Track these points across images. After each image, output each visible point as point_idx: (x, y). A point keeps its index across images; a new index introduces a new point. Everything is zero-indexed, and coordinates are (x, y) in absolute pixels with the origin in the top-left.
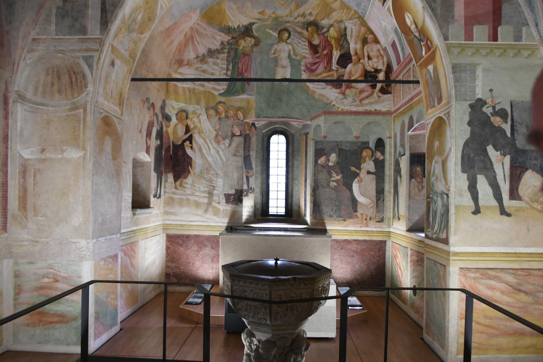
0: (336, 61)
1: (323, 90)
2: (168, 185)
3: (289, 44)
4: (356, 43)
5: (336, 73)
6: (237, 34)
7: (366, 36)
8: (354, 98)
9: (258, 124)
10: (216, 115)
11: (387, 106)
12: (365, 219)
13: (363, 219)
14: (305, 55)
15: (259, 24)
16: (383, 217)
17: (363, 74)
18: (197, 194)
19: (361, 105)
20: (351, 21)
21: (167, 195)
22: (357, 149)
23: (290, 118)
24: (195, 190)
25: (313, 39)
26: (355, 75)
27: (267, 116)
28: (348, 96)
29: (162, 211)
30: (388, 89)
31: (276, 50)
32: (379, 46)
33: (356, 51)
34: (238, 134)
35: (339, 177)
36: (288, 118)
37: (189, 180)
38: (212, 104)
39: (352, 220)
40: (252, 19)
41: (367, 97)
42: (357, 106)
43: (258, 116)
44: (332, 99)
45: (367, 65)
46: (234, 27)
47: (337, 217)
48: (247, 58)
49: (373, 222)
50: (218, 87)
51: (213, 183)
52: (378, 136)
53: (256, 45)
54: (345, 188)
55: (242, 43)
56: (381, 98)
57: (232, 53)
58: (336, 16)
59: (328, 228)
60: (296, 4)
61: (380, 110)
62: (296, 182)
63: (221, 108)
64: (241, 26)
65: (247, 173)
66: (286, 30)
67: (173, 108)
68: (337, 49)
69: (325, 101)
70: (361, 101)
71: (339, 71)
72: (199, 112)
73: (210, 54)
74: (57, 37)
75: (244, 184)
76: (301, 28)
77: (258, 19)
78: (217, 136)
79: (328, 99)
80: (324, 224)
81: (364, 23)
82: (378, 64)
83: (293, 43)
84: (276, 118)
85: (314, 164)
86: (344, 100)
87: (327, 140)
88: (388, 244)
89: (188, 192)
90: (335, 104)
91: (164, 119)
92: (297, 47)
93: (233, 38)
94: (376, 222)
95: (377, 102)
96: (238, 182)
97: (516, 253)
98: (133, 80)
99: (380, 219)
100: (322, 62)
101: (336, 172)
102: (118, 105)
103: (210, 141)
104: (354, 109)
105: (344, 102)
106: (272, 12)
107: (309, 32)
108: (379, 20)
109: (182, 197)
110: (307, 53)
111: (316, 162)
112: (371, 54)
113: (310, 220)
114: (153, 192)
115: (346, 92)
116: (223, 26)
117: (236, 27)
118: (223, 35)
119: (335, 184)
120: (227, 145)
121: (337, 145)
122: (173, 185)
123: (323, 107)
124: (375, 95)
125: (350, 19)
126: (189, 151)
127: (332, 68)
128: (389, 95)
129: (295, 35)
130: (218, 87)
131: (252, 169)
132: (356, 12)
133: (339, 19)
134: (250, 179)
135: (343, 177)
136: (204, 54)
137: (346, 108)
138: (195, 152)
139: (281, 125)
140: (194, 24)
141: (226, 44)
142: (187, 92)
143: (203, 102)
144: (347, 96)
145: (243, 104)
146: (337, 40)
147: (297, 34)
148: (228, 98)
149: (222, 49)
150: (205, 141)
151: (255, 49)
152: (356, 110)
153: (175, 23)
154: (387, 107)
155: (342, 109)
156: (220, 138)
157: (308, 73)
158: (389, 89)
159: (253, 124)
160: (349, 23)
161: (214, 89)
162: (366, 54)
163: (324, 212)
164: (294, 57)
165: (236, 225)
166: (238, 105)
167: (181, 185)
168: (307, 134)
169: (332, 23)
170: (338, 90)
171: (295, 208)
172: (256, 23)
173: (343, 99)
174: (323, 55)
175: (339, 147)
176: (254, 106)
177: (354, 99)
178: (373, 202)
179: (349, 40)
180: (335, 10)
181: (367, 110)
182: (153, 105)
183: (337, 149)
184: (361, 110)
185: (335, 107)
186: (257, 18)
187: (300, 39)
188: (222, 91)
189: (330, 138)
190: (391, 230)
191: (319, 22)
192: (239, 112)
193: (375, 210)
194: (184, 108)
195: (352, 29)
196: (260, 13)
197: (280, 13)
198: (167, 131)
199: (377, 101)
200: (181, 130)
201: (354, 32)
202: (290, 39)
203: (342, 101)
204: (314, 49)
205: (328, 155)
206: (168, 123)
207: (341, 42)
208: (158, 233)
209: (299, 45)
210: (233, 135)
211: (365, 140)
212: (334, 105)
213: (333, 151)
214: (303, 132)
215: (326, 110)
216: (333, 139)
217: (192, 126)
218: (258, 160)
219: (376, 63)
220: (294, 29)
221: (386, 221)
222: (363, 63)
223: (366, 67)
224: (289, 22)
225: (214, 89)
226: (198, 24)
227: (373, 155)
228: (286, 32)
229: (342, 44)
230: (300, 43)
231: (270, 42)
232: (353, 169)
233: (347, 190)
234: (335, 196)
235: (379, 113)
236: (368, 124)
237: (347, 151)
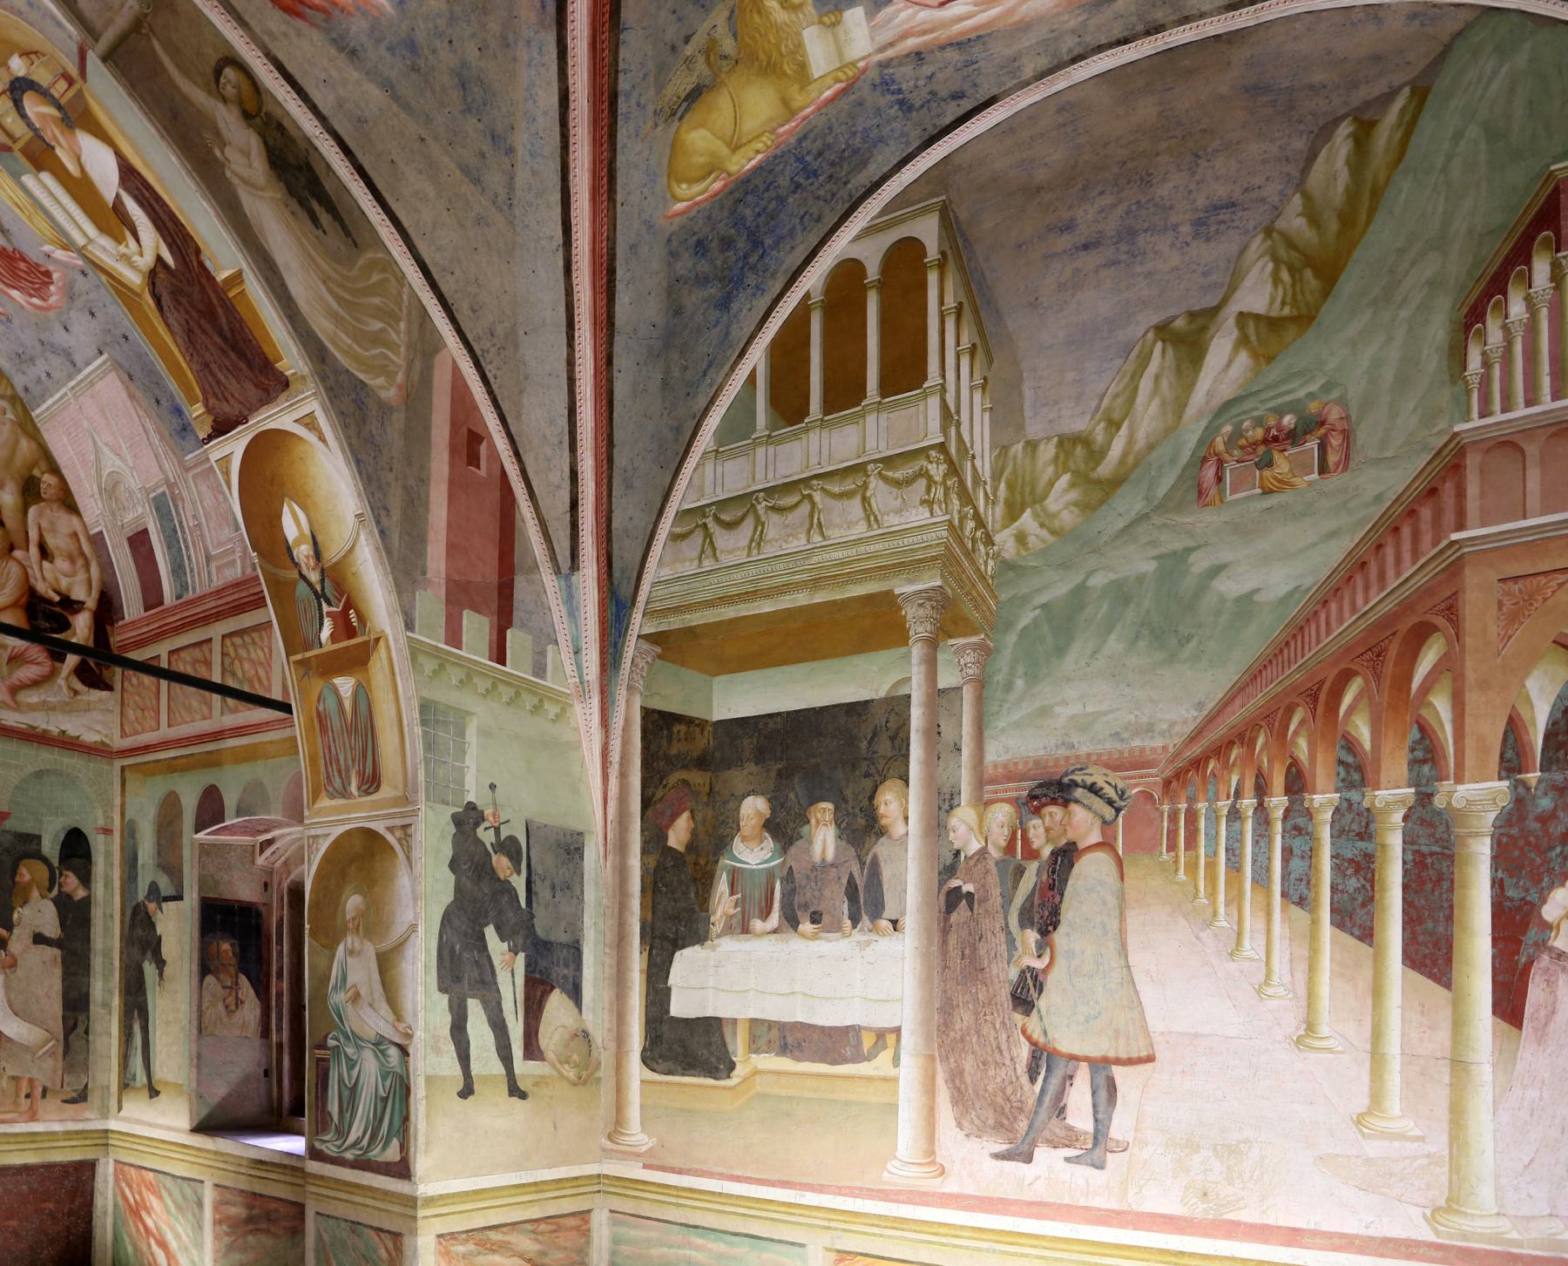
12: (28, 1096)
13: (17, 1096)
16: (86, 1086)
41: (35, 684)
45: (38, 575)
49: (52, 1105)
70: (14, 690)
88: (100, 1170)
94: (65, 1101)
97: (535, 1184)
108: (95, 442)
112: (51, 542)
178: (53, 1036)
184: (15, 724)
190: (113, 1125)
193: (60, 1064)
211: (28, 827)
221: (94, 1097)
223: (32, 580)
235: (71, 744)
236: (39, 774)
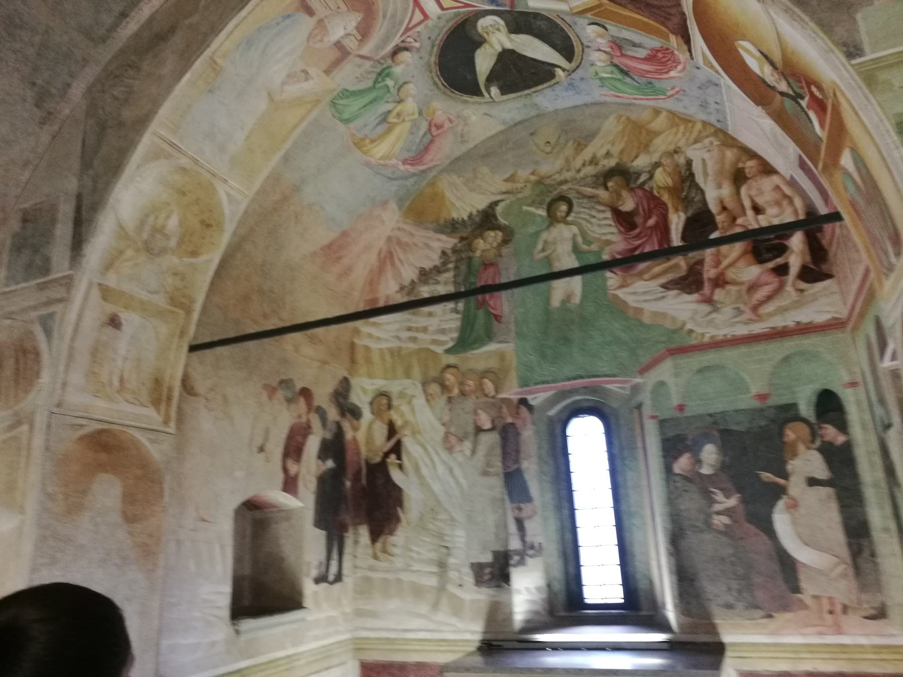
0: (680, 235)
2: (360, 551)
3: (572, 223)
4: (719, 186)
6: (469, 229)
7: (740, 165)
8: (738, 305)
9: (536, 399)
10: (443, 393)
11: (828, 309)
14: (609, 237)
15: (508, 202)
18: (416, 567)
20: (698, 145)
21: (360, 573)
22: (767, 426)
23: (594, 376)
24: (412, 558)
25: (620, 203)
27: (544, 379)
28: (722, 303)
29: (348, 609)
31: (546, 242)
32: (775, 179)
33: (722, 202)
34: (488, 425)
35: (733, 502)
36: (589, 377)
37: (399, 538)
38: (433, 373)
39: (788, 615)
40: (493, 194)
41: (769, 298)
42: (749, 323)
43: (524, 383)
46: (463, 219)
47: (747, 608)
48: (491, 270)
49: (853, 620)
50: (443, 338)
51: (445, 541)
52: (818, 386)
53: (506, 242)
54: (752, 529)
55: (480, 245)
56: (806, 293)
57: (463, 268)
58: (661, 145)
59: (727, 638)
60: (577, 143)
62: (636, 521)
63: (450, 377)
64: (475, 213)
65: (517, 511)
66: (563, 198)
67: (364, 391)
68: (677, 210)
69: (668, 325)
70: (755, 309)
72: (409, 392)
73: (423, 278)
74: (7, 289)
75: (511, 537)
76: (592, 188)
77: (505, 193)
78: (447, 435)
79: (674, 319)
80: (712, 629)
81: (728, 141)
83: (580, 221)
84: (564, 380)
85: (663, 476)
86: (714, 315)
87: (688, 413)
89: (399, 563)
91: (348, 415)
92: (589, 225)
93: (462, 239)
94: (867, 618)
95: (797, 305)
96: (497, 535)
98: (193, 348)
99: (873, 608)
101: (721, 489)
102: (150, 405)
103: (434, 449)
104: (742, 330)
105: (716, 318)
106: (530, 171)
107: (610, 189)
109: (387, 576)
110: (612, 233)
111: (668, 469)
112: (760, 201)
113: (677, 621)
114: (314, 573)
115: (716, 297)
116: (442, 221)
117: (466, 218)
118: (443, 237)
119: (725, 520)
120: (468, 452)
121: (715, 423)
122: (370, 551)
123: (663, 339)
124: (789, 288)
125: (696, 141)
126: (396, 475)
128: (827, 283)
129: (581, 203)
130: (443, 338)
131: (528, 499)
132: (705, 124)
133: (672, 148)
134: (529, 525)
135: (743, 501)
136: (413, 281)
137: (721, 333)
138: (406, 474)
139: (586, 394)
140: (392, 230)
141: (449, 252)
142: (388, 357)
143: (416, 371)
144: (719, 306)
145: (493, 363)
146: (674, 191)
147: (585, 201)
148: (462, 355)
149: (444, 264)
150: (425, 449)
151: (505, 251)
152: (749, 333)
153: (344, 234)
155: (712, 337)
156: (453, 440)
157: (619, 273)
158: (824, 267)
159: (523, 402)
160: (695, 149)
161: (435, 342)
162: (747, 204)
163: (711, 597)
164: (585, 247)
165: (501, 637)
166: (481, 365)
167: (385, 551)
168: (639, 407)
169: (657, 161)
170: (695, 297)
171: (642, 585)
172: (502, 200)
175: (722, 427)
176: (514, 363)
177: (738, 309)
179: (702, 185)
180: (657, 134)
182: (306, 393)
183: (716, 434)
185: (694, 335)
186: (504, 190)
187: (593, 208)
188: (451, 344)
189: (695, 408)
191: (629, 165)
192: (486, 380)
194: (384, 389)
195: (704, 160)
196: (507, 180)
197: (546, 169)
198: (355, 440)
199: (796, 302)
200: (380, 432)
201: (710, 164)
202: (573, 214)
204: (625, 220)
205: (695, 450)
206: (355, 422)
207: (684, 193)
208: (335, 661)
209: (593, 220)
210: (479, 430)
211: (785, 400)
212: (691, 331)
213: (706, 437)
214: (634, 403)
215: (672, 346)
216: (701, 411)
217: (399, 422)
218: (544, 478)
219: (777, 216)
220: (578, 192)
224: (565, 182)
225: (435, 342)
226: (399, 229)
227: (814, 435)
228: (561, 203)
229: (686, 197)
230: (594, 217)
231: (531, 230)
232: (767, 476)
233: (762, 534)
234: (730, 551)
235: (806, 329)
236: (786, 359)
237: (742, 432)
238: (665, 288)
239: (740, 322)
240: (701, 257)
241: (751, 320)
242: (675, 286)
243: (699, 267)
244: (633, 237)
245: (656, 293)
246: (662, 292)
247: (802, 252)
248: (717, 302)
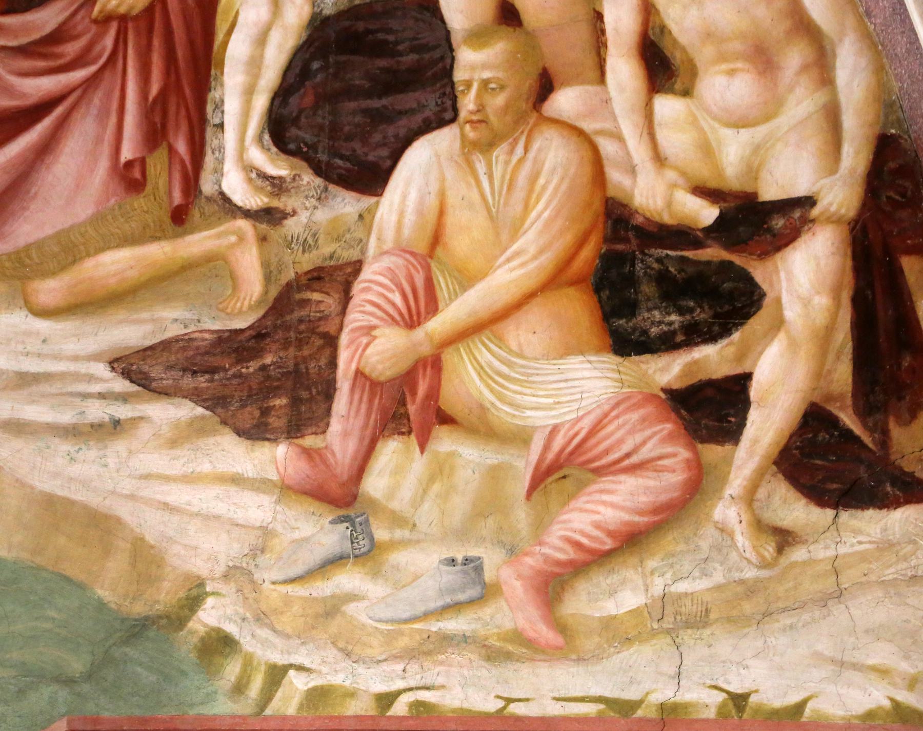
0: (261, 102)
1: (91, 453)
5: (263, 239)
8: (473, 552)
17: (588, 252)
19: (545, 634)
26: (481, 275)
28: (397, 520)
30: (885, 441)
42: (508, 656)
44: (199, 566)
56: (798, 554)
61: (800, 707)
71: (293, 226)
82: (760, 131)
90: (231, 629)
100: (97, 99)
105: (352, 597)
123: (77, 665)
127: (207, 186)
144: (381, 534)
152: (492, 705)
154: (882, 672)
155: (318, 695)
173: (334, 562)
174: (106, 20)
177: (473, 565)
181: (624, 708)
184: (555, 710)
185: (232, 670)
199: (750, 589)
203: (324, 588)
219: (740, 123)
222: (588, 126)
223: (616, 177)
238: (127, 374)
239: (464, 640)
240: (352, 254)
241: (518, 637)
242: (188, 382)
243: (328, 302)
244: (23, 51)
245: (85, 396)
246: (124, 398)
247: (825, 337)
248: (373, 503)
